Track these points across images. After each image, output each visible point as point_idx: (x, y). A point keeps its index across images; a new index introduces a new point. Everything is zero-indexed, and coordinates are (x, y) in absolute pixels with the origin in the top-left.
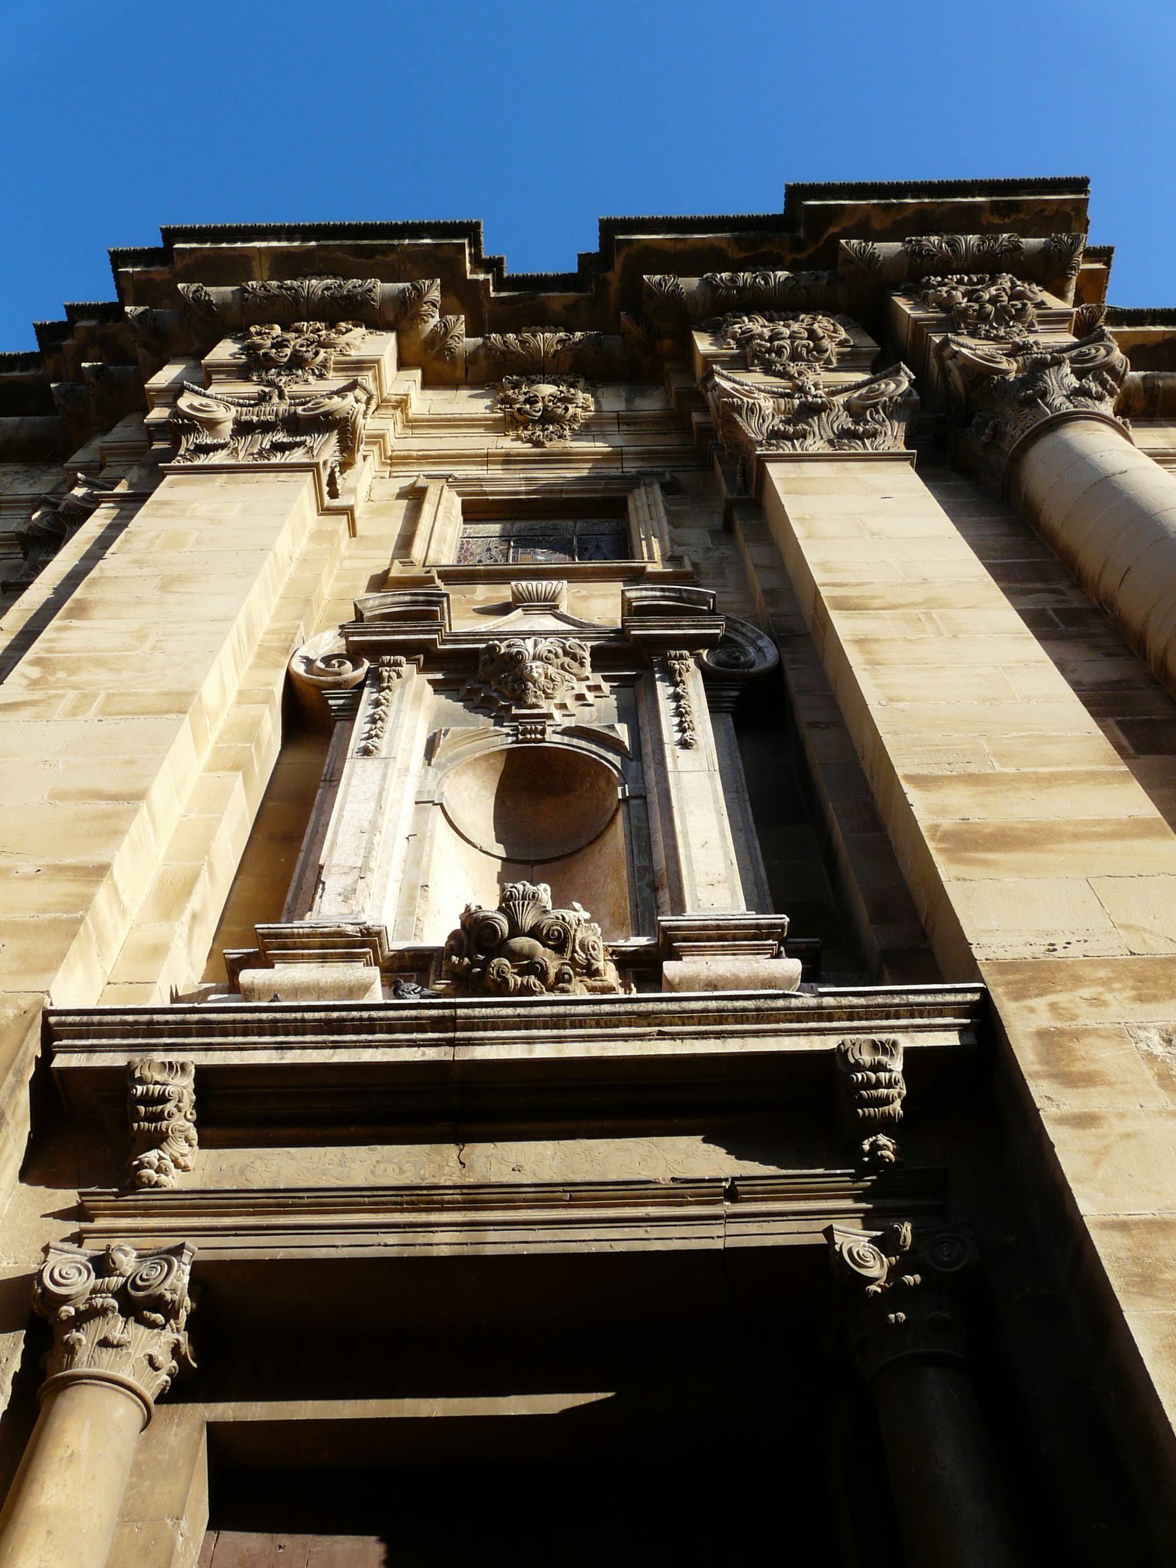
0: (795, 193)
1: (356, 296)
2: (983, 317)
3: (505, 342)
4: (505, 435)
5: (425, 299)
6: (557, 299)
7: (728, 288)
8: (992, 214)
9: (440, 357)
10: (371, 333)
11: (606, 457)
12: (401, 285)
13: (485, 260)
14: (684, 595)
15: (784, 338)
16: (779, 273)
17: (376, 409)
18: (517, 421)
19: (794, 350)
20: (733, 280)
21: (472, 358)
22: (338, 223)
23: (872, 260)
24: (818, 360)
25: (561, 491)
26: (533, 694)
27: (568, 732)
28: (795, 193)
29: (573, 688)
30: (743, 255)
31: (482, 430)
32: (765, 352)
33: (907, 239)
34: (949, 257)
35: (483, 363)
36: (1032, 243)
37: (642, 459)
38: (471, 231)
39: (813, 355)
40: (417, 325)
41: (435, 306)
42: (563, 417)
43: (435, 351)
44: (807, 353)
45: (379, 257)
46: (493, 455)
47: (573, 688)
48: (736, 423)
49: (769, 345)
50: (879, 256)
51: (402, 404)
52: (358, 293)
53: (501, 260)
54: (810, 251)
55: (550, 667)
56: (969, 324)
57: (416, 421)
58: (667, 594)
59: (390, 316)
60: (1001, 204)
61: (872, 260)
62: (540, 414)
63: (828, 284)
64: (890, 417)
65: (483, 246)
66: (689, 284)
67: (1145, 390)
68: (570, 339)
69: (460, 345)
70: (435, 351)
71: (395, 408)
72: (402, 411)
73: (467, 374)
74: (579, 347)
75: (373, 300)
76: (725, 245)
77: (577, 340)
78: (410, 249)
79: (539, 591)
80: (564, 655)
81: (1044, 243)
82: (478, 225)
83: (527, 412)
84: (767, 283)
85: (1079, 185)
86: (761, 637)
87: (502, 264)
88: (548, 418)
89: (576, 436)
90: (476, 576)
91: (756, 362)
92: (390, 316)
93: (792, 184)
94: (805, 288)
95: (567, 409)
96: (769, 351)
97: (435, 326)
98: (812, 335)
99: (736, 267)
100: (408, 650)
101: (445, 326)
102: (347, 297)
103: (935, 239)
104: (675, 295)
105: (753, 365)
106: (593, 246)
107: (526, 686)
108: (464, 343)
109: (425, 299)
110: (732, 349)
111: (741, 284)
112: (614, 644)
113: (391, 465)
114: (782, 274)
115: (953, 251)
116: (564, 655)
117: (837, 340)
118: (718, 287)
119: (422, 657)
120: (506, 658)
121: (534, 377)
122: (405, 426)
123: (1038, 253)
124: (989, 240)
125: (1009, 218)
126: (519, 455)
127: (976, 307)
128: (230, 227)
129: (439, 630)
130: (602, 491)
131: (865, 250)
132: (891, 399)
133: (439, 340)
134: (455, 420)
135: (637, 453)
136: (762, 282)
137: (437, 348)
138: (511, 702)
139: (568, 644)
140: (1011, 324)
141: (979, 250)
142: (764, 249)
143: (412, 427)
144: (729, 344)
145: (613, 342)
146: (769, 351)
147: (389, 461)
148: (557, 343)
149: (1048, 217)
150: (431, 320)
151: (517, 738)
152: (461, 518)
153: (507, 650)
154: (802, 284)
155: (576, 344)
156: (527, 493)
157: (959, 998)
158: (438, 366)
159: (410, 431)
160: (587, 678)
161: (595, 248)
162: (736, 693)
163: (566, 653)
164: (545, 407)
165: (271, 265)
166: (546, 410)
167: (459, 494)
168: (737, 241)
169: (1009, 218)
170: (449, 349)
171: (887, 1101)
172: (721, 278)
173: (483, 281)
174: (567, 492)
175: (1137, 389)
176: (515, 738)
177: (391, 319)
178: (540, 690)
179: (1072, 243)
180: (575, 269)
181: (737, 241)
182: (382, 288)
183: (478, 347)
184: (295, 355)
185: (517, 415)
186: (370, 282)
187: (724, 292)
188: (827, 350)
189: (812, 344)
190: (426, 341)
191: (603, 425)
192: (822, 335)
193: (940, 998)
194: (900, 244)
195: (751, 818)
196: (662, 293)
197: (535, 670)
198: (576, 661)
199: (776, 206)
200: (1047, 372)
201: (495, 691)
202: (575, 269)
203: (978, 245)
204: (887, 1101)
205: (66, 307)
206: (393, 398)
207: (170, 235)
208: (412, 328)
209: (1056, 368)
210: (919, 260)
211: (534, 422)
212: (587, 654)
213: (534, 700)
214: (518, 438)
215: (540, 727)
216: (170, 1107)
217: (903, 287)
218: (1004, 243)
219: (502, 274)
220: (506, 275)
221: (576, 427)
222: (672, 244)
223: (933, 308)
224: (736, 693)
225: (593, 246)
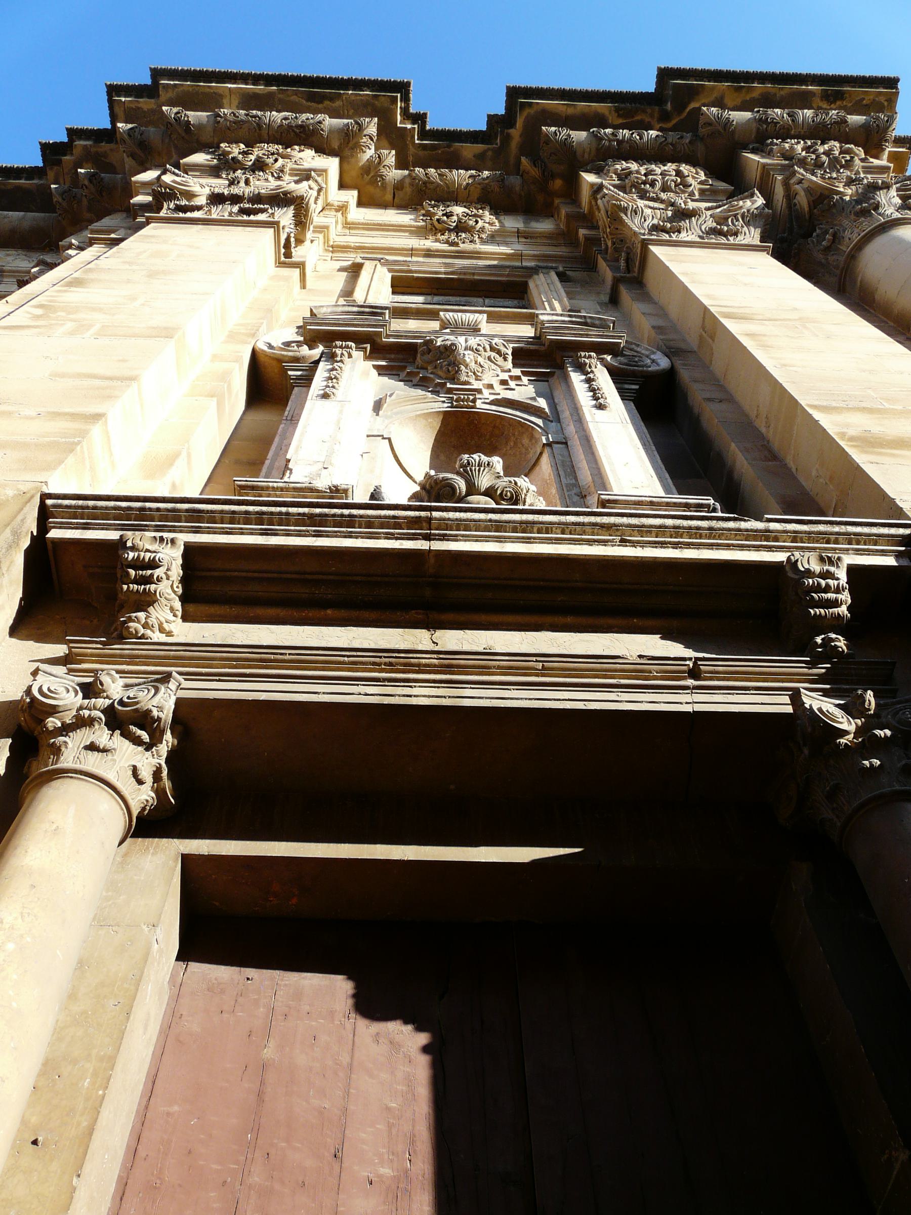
0: (665, 74)
1: (308, 126)
3: (426, 174)
4: (426, 239)
5: (365, 133)
6: (469, 150)
7: (610, 140)
8: (822, 100)
9: (373, 182)
10: (319, 156)
11: (509, 257)
12: (346, 121)
13: (412, 114)
14: (589, 320)
15: (656, 175)
16: (651, 132)
17: (321, 211)
18: (436, 229)
21: (399, 186)
22: (295, 74)
23: (727, 123)
24: (684, 192)
25: (474, 274)
26: (466, 374)
27: (493, 403)
28: (665, 74)
29: (498, 376)
31: (407, 234)
32: (641, 184)
33: (756, 110)
34: (789, 125)
35: (408, 189)
36: (856, 119)
37: (539, 260)
38: (403, 88)
39: (680, 189)
40: (357, 153)
41: (372, 140)
42: (473, 227)
43: (370, 176)
44: (675, 186)
45: (327, 103)
46: (416, 250)
47: (498, 376)
48: (622, 222)
49: (644, 178)
50: (733, 121)
51: (342, 208)
52: (310, 124)
53: (425, 115)
54: (674, 122)
55: (479, 357)
57: (353, 223)
58: (574, 319)
59: (335, 145)
60: (830, 92)
61: (727, 123)
62: (455, 224)
63: (690, 142)
64: (748, 224)
65: (411, 102)
66: (579, 136)
68: (479, 175)
69: (390, 174)
70: (370, 176)
71: (337, 211)
72: (342, 214)
73: (394, 198)
74: (487, 182)
75: (322, 130)
76: (607, 113)
77: (485, 176)
78: (353, 98)
79: (464, 320)
80: (490, 351)
81: (865, 119)
82: (408, 84)
83: (444, 222)
84: (641, 138)
85: (891, 83)
86: (654, 353)
87: (426, 118)
88: (461, 228)
89: (483, 242)
90: (408, 313)
91: (634, 190)
92: (335, 145)
93: (663, 67)
94: (671, 144)
95: (477, 222)
96: (644, 183)
97: (371, 157)
98: (679, 173)
99: (616, 127)
100: (359, 339)
101: (379, 157)
102: (301, 126)
103: (778, 111)
104: (566, 145)
106: (500, 109)
107: (459, 368)
108: (394, 174)
109: (365, 133)
110: (615, 180)
111: (621, 138)
112: (532, 347)
113: (332, 252)
114: (653, 133)
115: (793, 121)
116: (490, 351)
117: (699, 180)
118: (601, 139)
119: (368, 346)
120: (442, 349)
121: (449, 203)
122: (344, 227)
123: (860, 126)
124: (822, 114)
125: (835, 104)
126: (437, 251)
127: (814, 157)
128: (207, 71)
129: (384, 325)
130: (508, 275)
131: (721, 116)
132: (748, 211)
133: (372, 169)
134: (385, 225)
135: (534, 256)
136: (638, 137)
137: (372, 174)
138: (446, 381)
139: (493, 342)
140: (841, 171)
141: (813, 121)
143: (350, 228)
144: (611, 177)
145: (515, 181)
146: (644, 183)
147: (331, 249)
148: (469, 178)
149: (866, 105)
150: (368, 150)
151: (452, 404)
152: (390, 290)
153: (442, 343)
154: (670, 140)
155: (484, 179)
156: (445, 273)
157: (893, 531)
158: (371, 189)
159: (347, 231)
160: (509, 371)
161: (501, 110)
162: (637, 387)
163: (492, 349)
164: (459, 221)
165: (239, 104)
166: (460, 222)
167: (390, 271)
168: (617, 110)
169: (835, 104)
170: (381, 176)
171: (836, 604)
172: (605, 133)
173: (410, 129)
174: (479, 274)
176: (450, 405)
177: (336, 147)
178: (471, 372)
179: (887, 121)
180: (484, 128)
182: (329, 123)
183: (405, 176)
184: (258, 161)
185: (436, 223)
186: (320, 117)
187: (607, 143)
188: (691, 185)
189: (679, 180)
190: (362, 167)
191: (505, 236)
192: (687, 174)
193: (875, 530)
194: (750, 113)
195: (659, 461)
196: (557, 141)
197: (467, 356)
198: (500, 356)
199: (648, 85)
200: (878, 193)
201: (431, 373)
202: (484, 128)
203: (813, 117)
204: (836, 604)
205: (67, 129)
206: (336, 204)
207: (157, 74)
208: (352, 156)
209: (885, 191)
210: (765, 126)
211: (450, 230)
212: (510, 352)
213: (466, 378)
214: (437, 241)
215: (471, 397)
216: (158, 572)
217: (751, 147)
218: (834, 117)
219: (425, 126)
220: (428, 128)
221: (484, 236)
222: (564, 109)
223: (778, 157)
224: (637, 387)
225: (500, 109)
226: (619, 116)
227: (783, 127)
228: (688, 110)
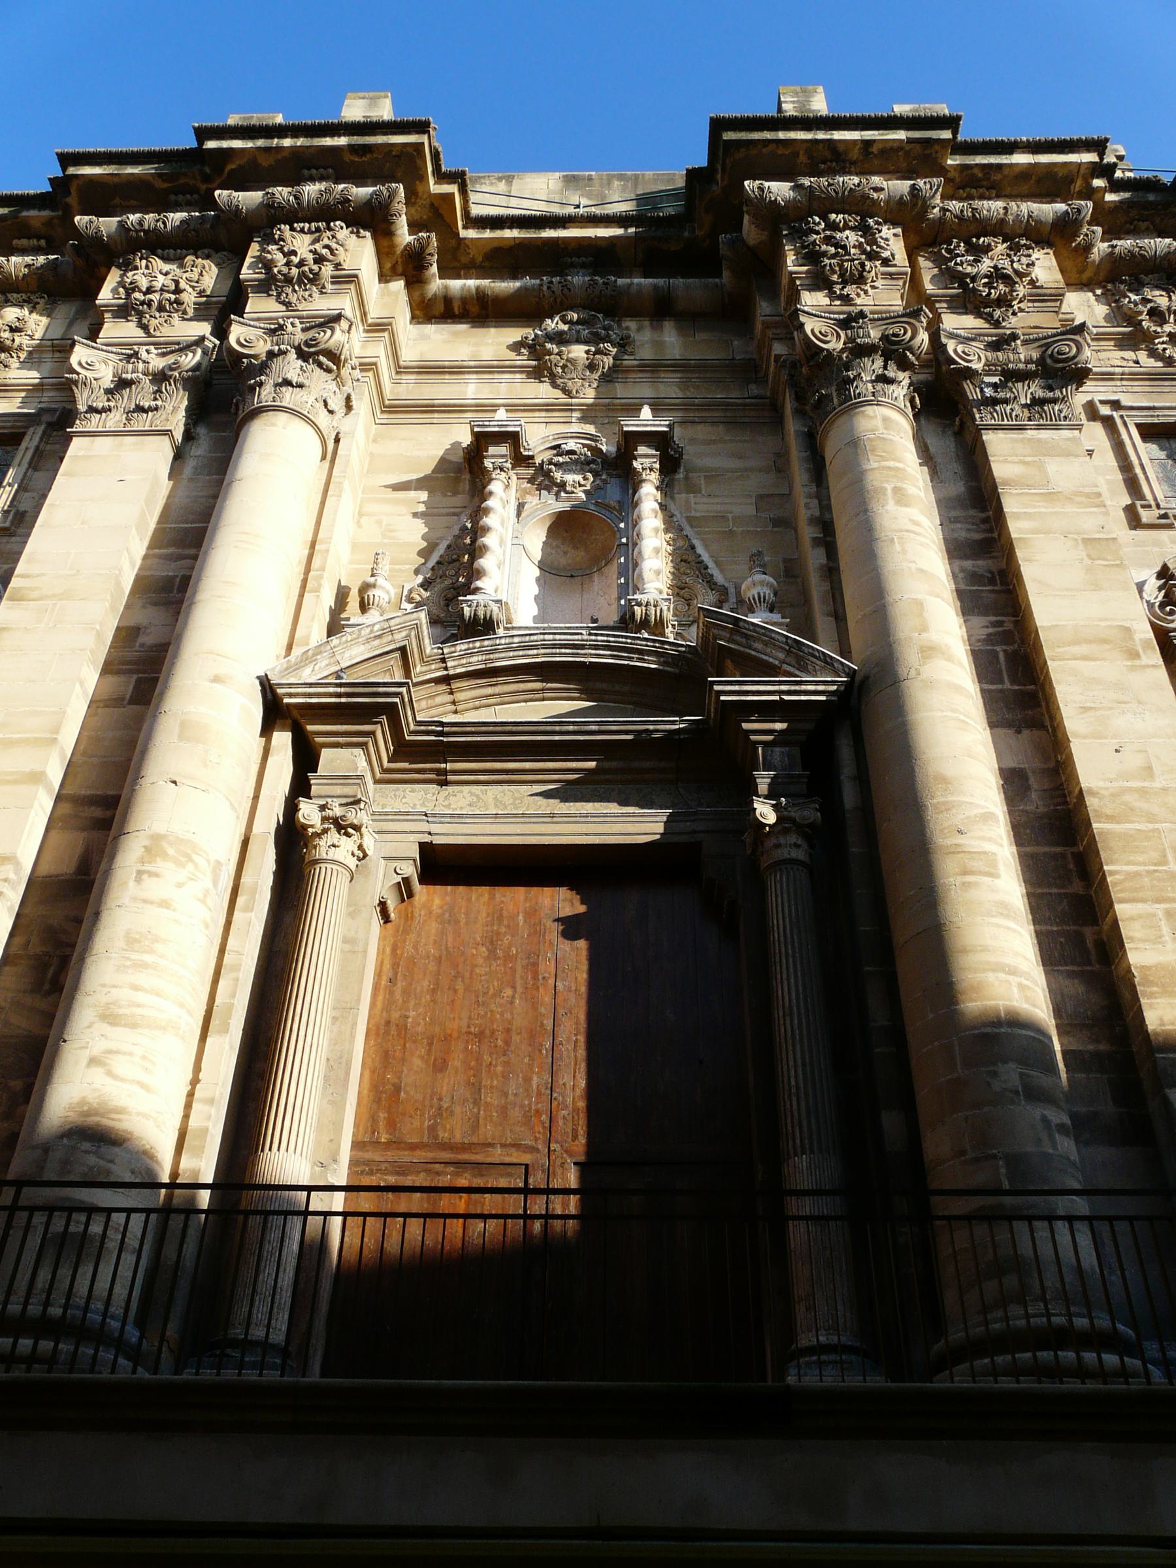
0: (203, 134)
2: (288, 280)
7: (137, 231)
19: (160, 302)
20: (141, 223)
24: (177, 311)
30: (166, 185)
36: (362, 192)
56: (279, 286)
67: (478, 298)
76: (151, 179)
77: (39, 265)
84: (165, 226)
94: (194, 230)
105: (131, 315)
110: (121, 298)
111: (146, 228)
115: (298, 204)
130: (12, 427)
135: (53, 385)
136: (162, 226)
140: (308, 287)
142: (182, 181)
146: (143, 303)
154: (192, 227)
175: (472, 297)
181: (160, 175)
187: (134, 234)
191: (42, 352)
196: (88, 236)
199: (191, 143)
210: (273, 211)
218: (337, 196)
226: (164, 181)
227: (289, 211)
228: (226, 171)
